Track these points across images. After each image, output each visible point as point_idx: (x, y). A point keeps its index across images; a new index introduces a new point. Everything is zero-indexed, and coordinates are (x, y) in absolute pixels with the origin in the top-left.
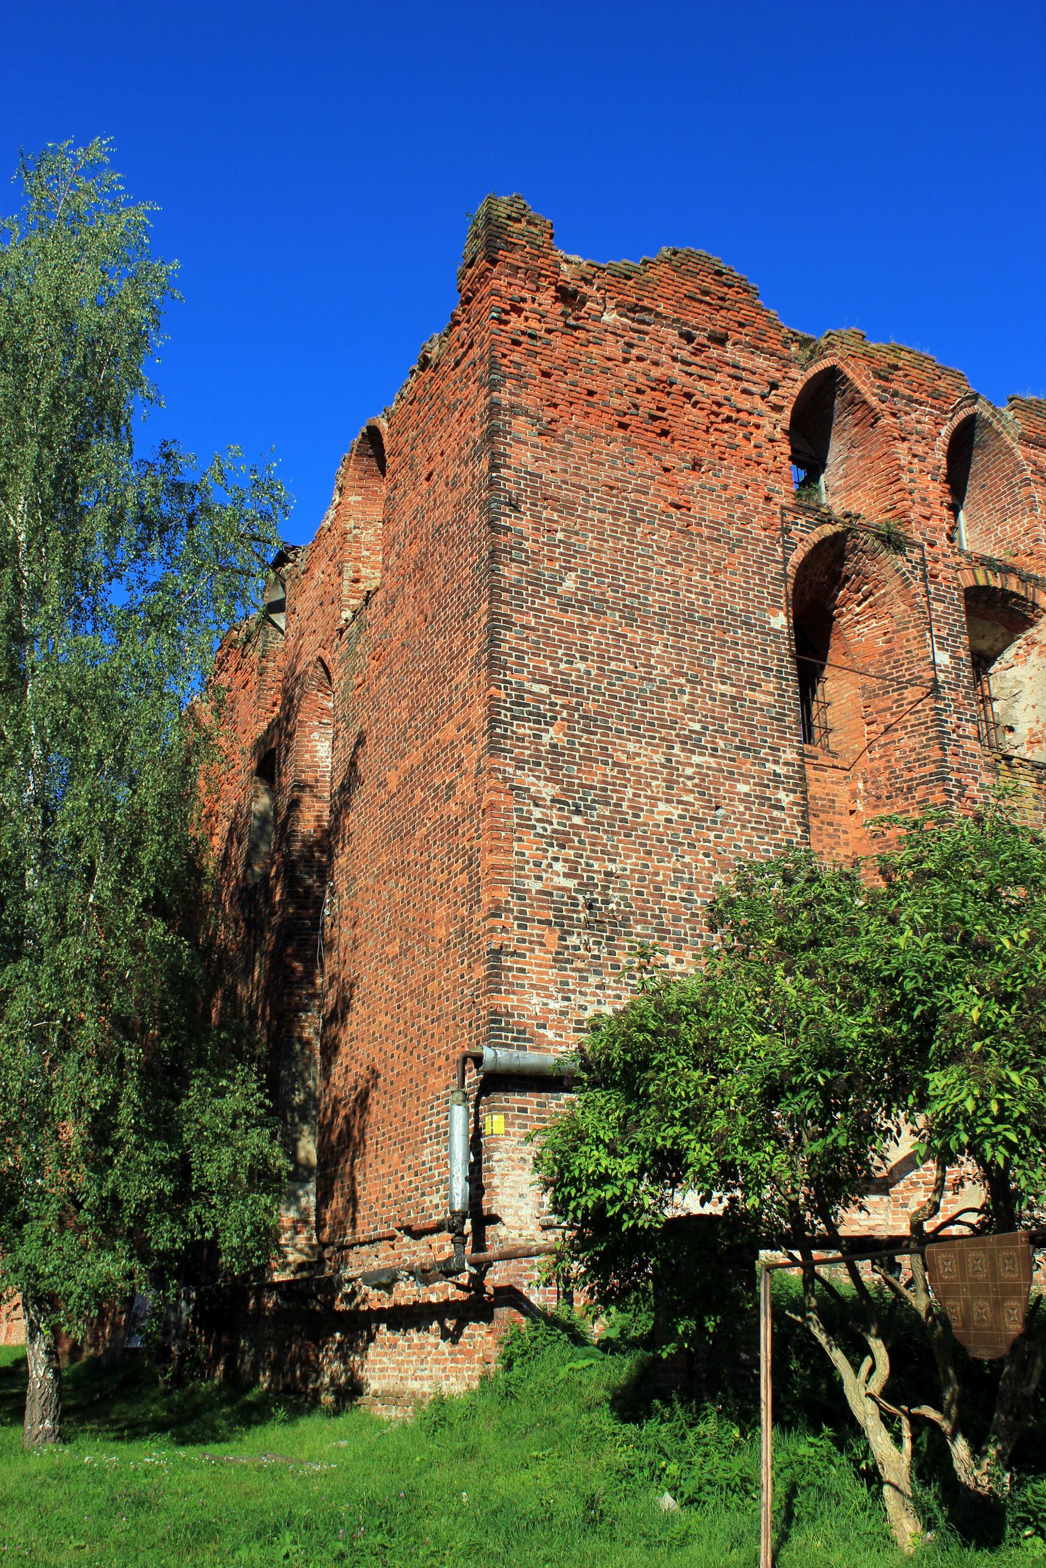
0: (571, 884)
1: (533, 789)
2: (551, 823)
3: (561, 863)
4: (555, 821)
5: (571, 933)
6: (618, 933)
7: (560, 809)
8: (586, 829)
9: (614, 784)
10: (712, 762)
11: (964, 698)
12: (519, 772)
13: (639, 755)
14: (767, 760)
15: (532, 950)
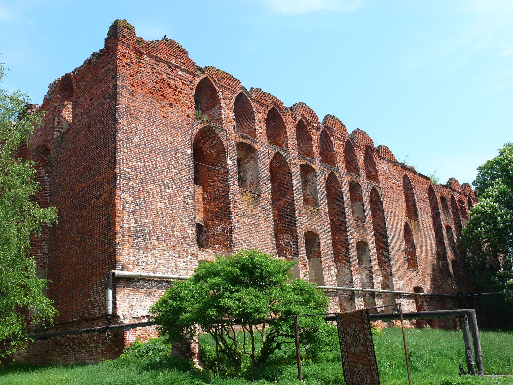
0: (136, 225)
1: (126, 199)
2: (131, 208)
3: (133, 220)
4: (132, 208)
5: (136, 239)
6: (147, 239)
7: (133, 205)
8: (140, 210)
9: (147, 197)
10: (172, 191)
12: (123, 194)
13: (153, 189)
15: (126, 244)
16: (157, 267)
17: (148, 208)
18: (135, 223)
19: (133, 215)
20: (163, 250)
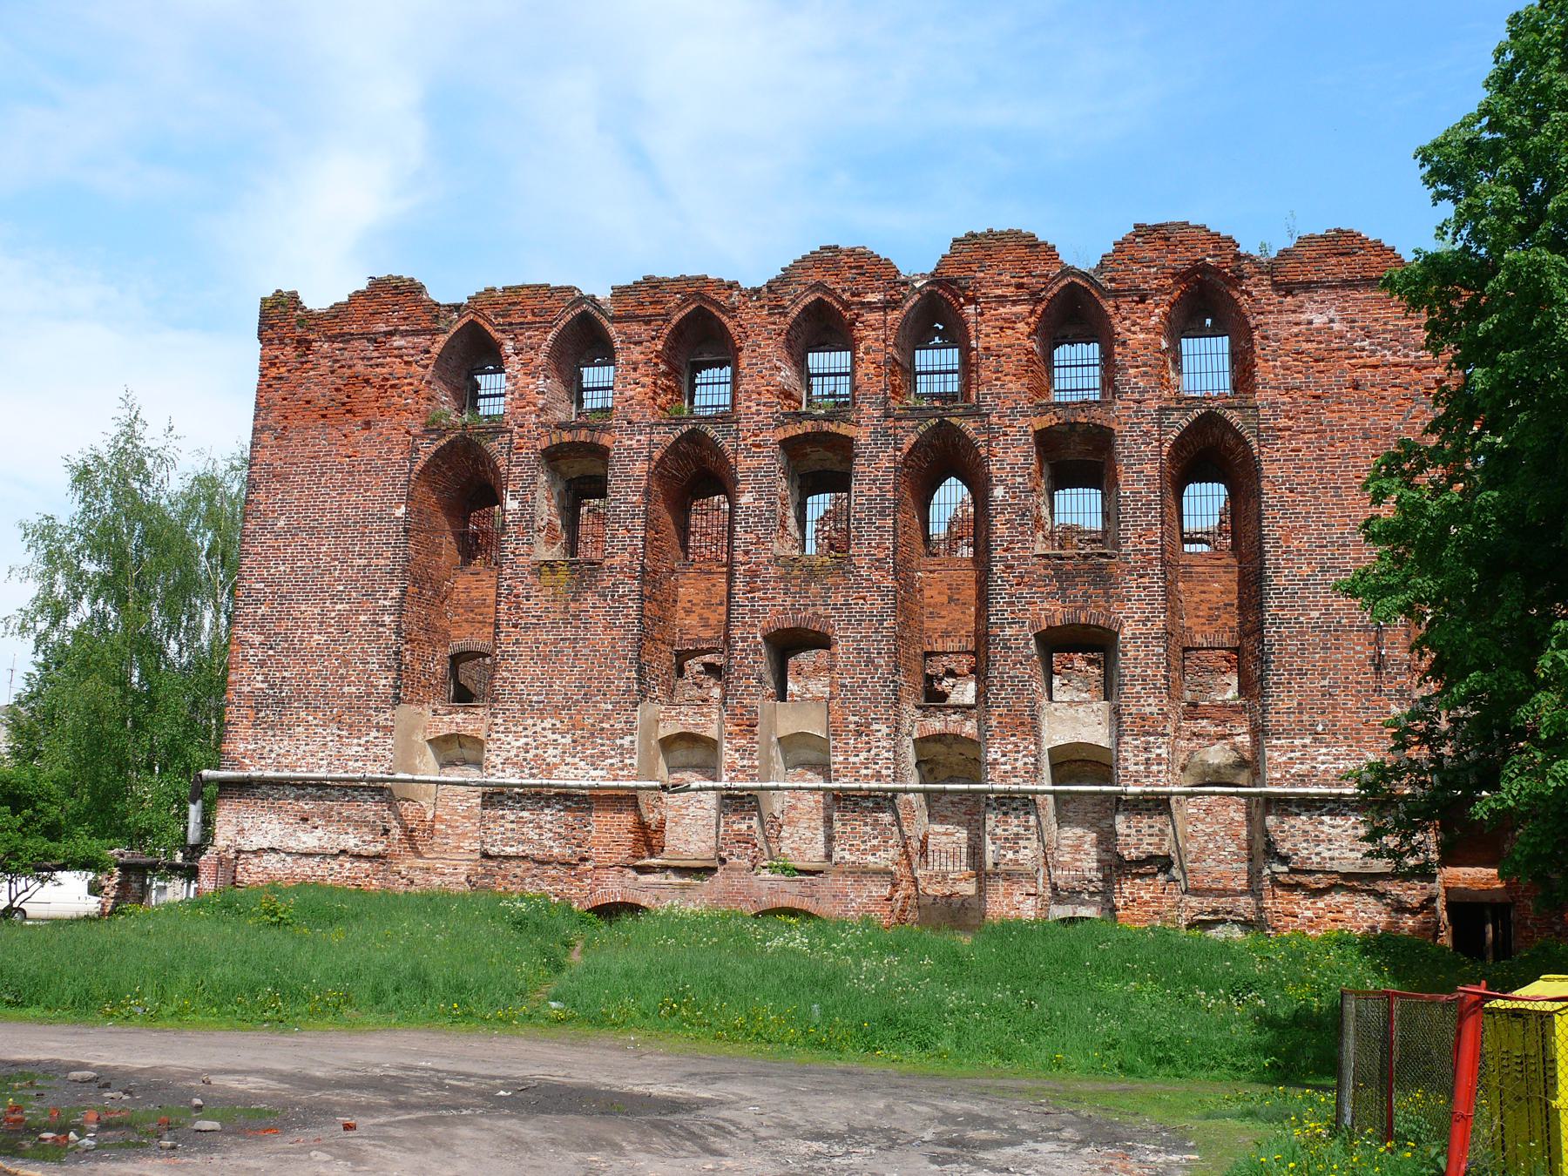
5: (261, 711)
6: (285, 708)
10: (347, 607)
16: (299, 759)
17: (292, 650)
18: (262, 682)
20: (316, 725)
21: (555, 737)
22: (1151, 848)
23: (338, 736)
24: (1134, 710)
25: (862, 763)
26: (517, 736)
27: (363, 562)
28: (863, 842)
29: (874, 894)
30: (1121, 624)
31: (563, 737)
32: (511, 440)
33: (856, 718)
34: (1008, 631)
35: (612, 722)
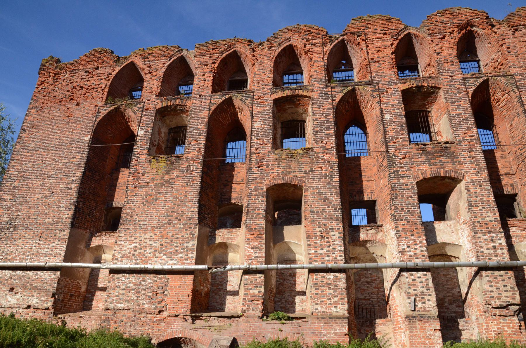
0: (7, 219)
10: (55, 181)
11: (145, 143)
13: (35, 184)
14: (71, 177)
18: (7, 218)
19: (8, 211)
21: (151, 243)
22: (508, 299)
23: (39, 244)
24: (480, 219)
25: (325, 254)
26: (131, 242)
27: (66, 161)
28: (328, 299)
29: (338, 331)
30: (464, 176)
31: (155, 243)
32: (144, 106)
33: (321, 229)
34: (402, 181)
35: (182, 234)
